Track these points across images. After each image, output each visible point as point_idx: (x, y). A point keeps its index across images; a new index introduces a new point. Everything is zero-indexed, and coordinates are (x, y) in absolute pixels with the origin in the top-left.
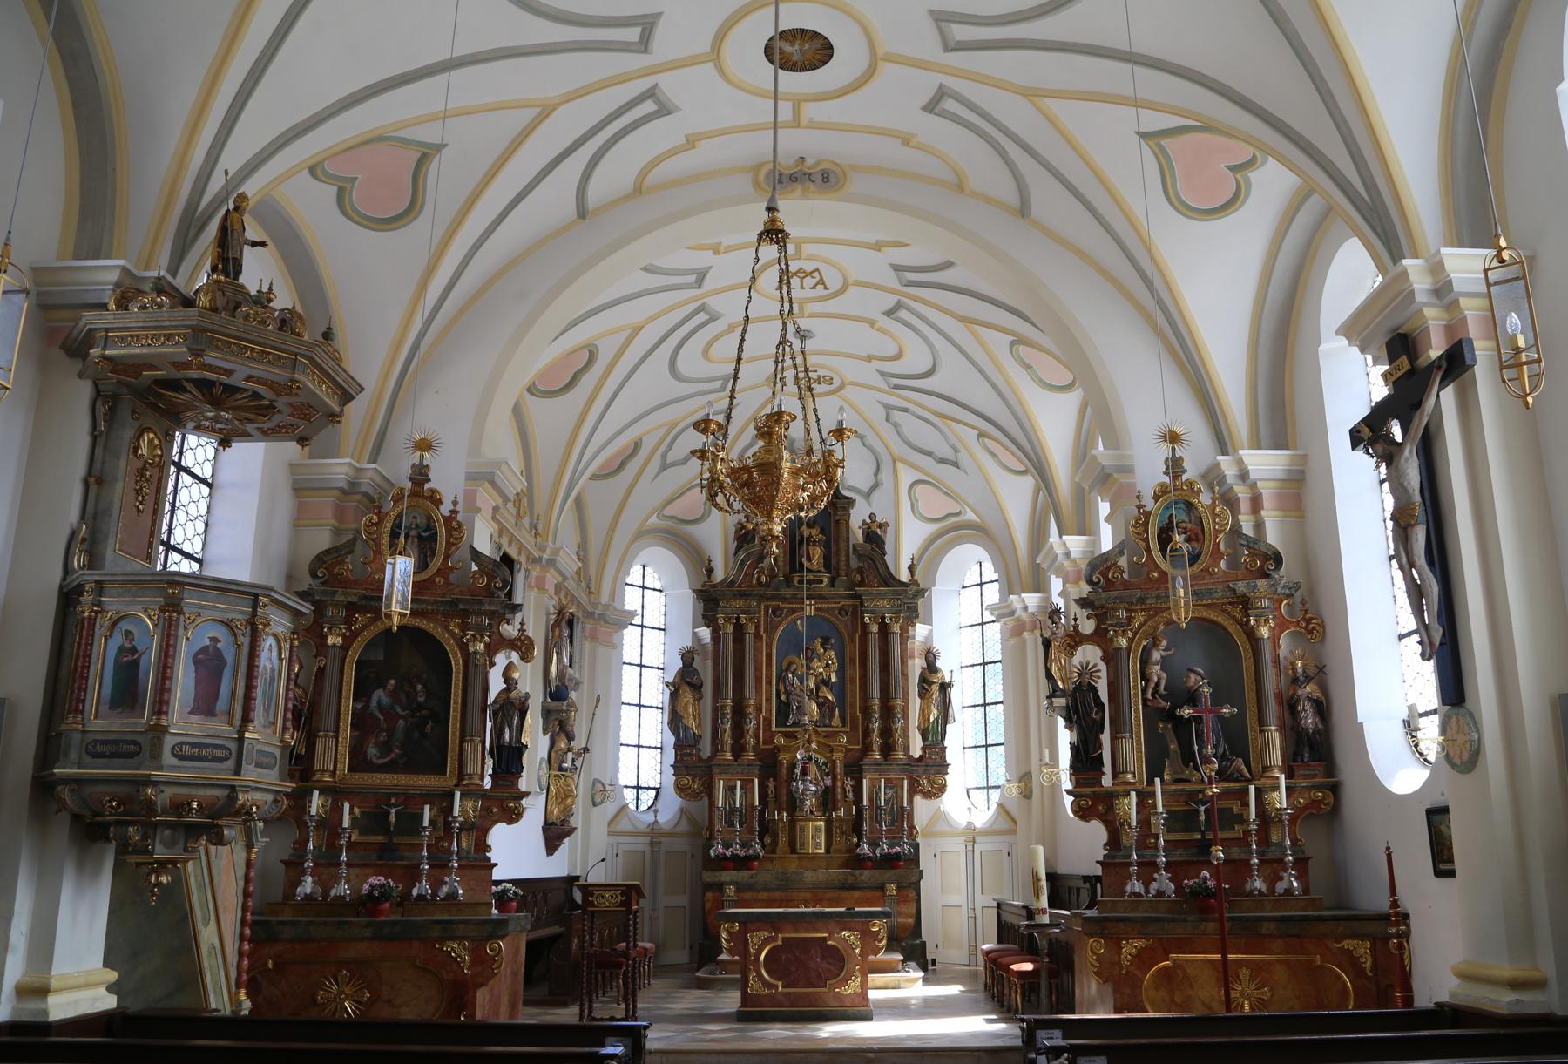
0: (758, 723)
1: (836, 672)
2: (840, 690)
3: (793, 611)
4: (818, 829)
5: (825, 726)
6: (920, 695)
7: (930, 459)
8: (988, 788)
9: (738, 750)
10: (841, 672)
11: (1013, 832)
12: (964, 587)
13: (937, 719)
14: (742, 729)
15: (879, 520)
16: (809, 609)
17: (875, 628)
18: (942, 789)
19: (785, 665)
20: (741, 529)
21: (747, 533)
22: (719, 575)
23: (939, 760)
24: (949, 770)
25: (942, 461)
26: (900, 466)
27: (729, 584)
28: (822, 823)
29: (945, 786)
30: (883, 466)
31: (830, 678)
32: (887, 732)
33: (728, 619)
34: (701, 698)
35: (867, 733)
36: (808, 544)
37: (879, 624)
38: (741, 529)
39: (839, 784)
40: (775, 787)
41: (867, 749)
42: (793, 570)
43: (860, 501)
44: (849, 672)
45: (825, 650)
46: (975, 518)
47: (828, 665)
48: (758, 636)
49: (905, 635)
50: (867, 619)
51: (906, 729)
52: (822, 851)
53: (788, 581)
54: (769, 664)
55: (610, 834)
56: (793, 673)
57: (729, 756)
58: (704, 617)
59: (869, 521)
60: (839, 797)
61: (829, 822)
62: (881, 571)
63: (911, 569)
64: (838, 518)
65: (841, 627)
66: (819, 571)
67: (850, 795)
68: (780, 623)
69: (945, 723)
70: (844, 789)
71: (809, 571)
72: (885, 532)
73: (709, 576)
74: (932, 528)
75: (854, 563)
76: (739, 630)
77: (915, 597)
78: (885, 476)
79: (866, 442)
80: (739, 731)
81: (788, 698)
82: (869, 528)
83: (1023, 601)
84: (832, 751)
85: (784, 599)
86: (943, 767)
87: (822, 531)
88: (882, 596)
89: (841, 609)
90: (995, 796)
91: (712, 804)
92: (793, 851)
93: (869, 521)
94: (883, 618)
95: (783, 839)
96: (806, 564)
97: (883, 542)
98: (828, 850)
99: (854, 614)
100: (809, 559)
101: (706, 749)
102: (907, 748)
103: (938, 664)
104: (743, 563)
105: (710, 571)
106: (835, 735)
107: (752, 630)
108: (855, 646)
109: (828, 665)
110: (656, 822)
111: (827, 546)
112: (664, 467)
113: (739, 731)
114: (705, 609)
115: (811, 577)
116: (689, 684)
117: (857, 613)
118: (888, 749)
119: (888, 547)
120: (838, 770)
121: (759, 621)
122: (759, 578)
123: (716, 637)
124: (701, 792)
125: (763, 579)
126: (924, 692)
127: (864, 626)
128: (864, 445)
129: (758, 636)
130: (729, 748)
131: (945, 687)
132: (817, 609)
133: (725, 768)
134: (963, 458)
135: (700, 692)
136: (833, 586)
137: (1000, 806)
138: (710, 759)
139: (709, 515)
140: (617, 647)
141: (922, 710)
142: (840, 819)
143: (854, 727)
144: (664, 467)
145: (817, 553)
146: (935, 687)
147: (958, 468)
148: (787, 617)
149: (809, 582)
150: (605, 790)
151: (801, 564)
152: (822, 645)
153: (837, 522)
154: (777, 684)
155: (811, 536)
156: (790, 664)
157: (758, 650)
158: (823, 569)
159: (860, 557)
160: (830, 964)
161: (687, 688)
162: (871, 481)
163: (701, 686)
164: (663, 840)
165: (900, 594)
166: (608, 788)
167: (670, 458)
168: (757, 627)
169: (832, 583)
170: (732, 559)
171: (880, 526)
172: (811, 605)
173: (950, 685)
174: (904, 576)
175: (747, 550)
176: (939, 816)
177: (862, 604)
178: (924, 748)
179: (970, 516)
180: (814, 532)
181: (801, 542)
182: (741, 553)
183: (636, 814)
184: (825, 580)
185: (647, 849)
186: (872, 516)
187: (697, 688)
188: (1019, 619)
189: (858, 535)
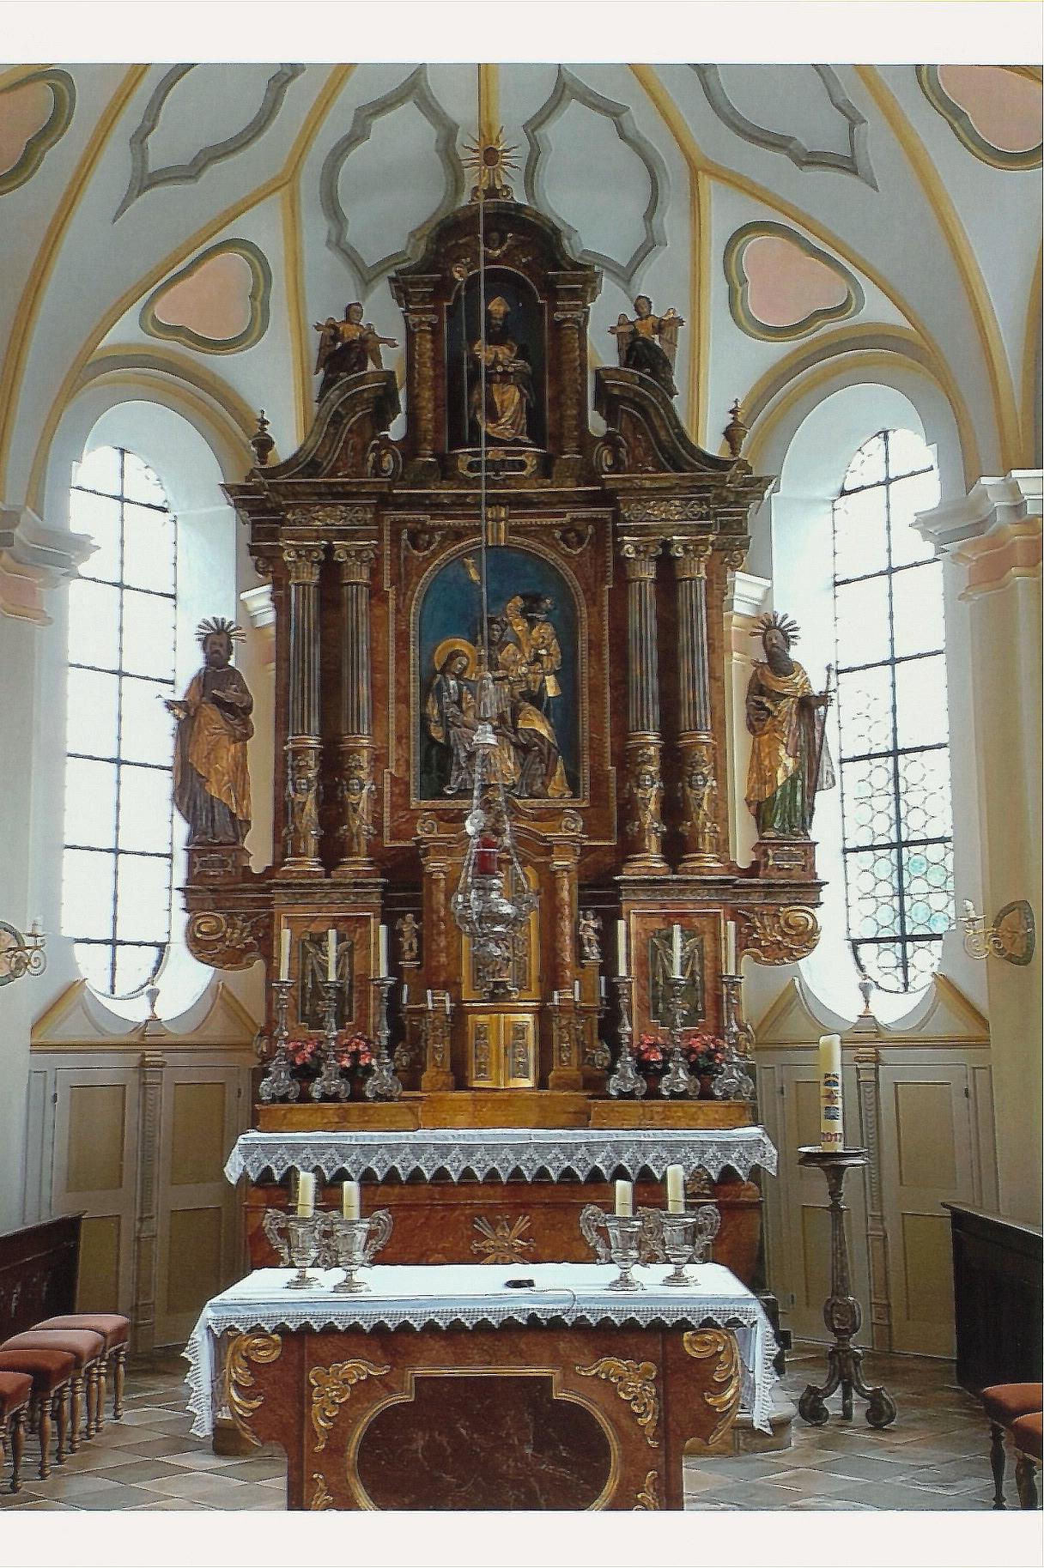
0: (380, 792)
1: (556, 673)
2: (564, 714)
3: (458, 535)
4: (520, 1031)
5: (532, 796)
6: (751, 727)
7: (782, 157)
8: (904, 939)
9: (332, 852)
10: (567, 674)
11: (983, 1042)
12: (843, 493)
13: (792, 779)
14: (343, 804)
15: (657, 312)
16: (497, 529)
17: (648, 572)
18: (807, 938)
19: (439, 659)
20: (335, 339)
21: (348, 347)
22: (287, 442)
23: (797, 872)
24: (823, 896)
25: (811, 160)
26: (707, 184)
27: (304, 463)
28: (529, 1018)
29: (815, 931)
30: (664, 191)
31: (543, 689)
32: (674, 809)
33: (303, 554)
34: (247, 736)
35: (629, 809)
36: (490, 380)
37: (658, 559)
38: (335, 339)
39: (567, 926)
40: (419, 935)
41: (629, 847)
42: (457, 442)
43: (607, 283)
44: (584, 669)
45: (532, 622)
46: (891, 316)
47: (538, 658)
48: (376, 593)
49: (718, 593)
50: (629, 551)
51: (720, 802)
52: (528, 1083)
53: (445, 468)
54: (402, 658)
55: (38, 1048)
56: (458, 677)
57: (312, 864)
58: (253, 551)
59: (632, 316)
60: (568, 957)
61: (543, 1015)
62: (663, 434)
63: (731, 435)
64: (559, 316)
65: (567, 572)
66: (517, 442)
67: (593, 952)
68: (428, 561)
69: (813, 789)
70: (578, 942)
71: (491, 441)
72: (672, 343)
73: (263, 457)
74: (779, 350)
75: (596, 423)
76: (331, 571)
77: (741, 499)
78: (672, 221)
79: (626, 125)
80: (333, 808)
81: (447, 735)
82: (634, 333)
83: (1014, 489)
84: (548, 851)
85: (433, 505)
86: (808, 889)
87: (522, 354)
88: (662, 495)
89: (566, 529)
90: (926, 960)
91: (272, 972)
92: (461, 1084)
93: (632, 316)
94: (667, 545)
95: (438, 1055)
96: (485, 427)
97: (667, 365)
98: (542, 1083)
99: (598, 543)
100: (493, 415)
101: (258, 852)
102: (722, 846)
103: (794, 653)
104: (336, 420)
105: (264, 444)
106: (555, 814)
107: (364, 577)
108: (600, 613)
109: (538, 658)
110: (154, 1018)
111: (531, 384)
112: (144, 181)
113: (333, 808)
114: (257, 534)
115: (496, 453)
116: (218, 702)
117: (604, 537)
118: (677, 848)
119: (678, 379)
120: (565, 895)
121: (379, 558)
122: (378, 461)
123: (280, 603)
124: (249, 948)
125: (388, 462)
126: (759, 718)
127: (621, 562)
128: (622, 136)
129: (376, 593)
130: (312, 845)
131: (810, 706)
132: (513, 530)
133: (303, 889)
134: (877, 144)
135: (246, 723)
136: (548, 475)
137: (943, 982)
138: (269, 872)
139: (265, 327)
140: (53, 621)
141: (756, 754)
142: (567, 1008)
143: (598, 797)
144: (144, 181)
145: (510, 398)
146: (789, 706)
147: (856, 173)
148: (442, 548)
149: (494, 466)
150: (22, 948)
151: (475, 427)
152: (524, 612)
153: (557, 326)
154: (423, 703)
155: (496, 362)
156: (453, 656)
157: (376, 624)
158: (525, 438)
159: (608, 403)
160: (564, 1462)
161: (211, 712)
162: (635, 235)
163: (248, 709)
164: (166, 1058)
165: (707, 489)
166: (29, 941)
167: (160, 153)
168: (375, 573)
169: (546, 467)
170: (315, 407)
171: (660, 328)
172: (498, 520)
173: (824, 699)
174: (711, 442)
175: (349, 386)
176: (793, 999)
177: (617, 516)
178: (761, 848)
179: (877, 309)
180: (503, 353)
181: (474, 378)
182: (333, 394)
183: (108, 1003)
184: (531, 462)
185: (132, 1080)
186: (641, 305)
187: (238, 712)
188: (994, 542)
189: (602, 351)
